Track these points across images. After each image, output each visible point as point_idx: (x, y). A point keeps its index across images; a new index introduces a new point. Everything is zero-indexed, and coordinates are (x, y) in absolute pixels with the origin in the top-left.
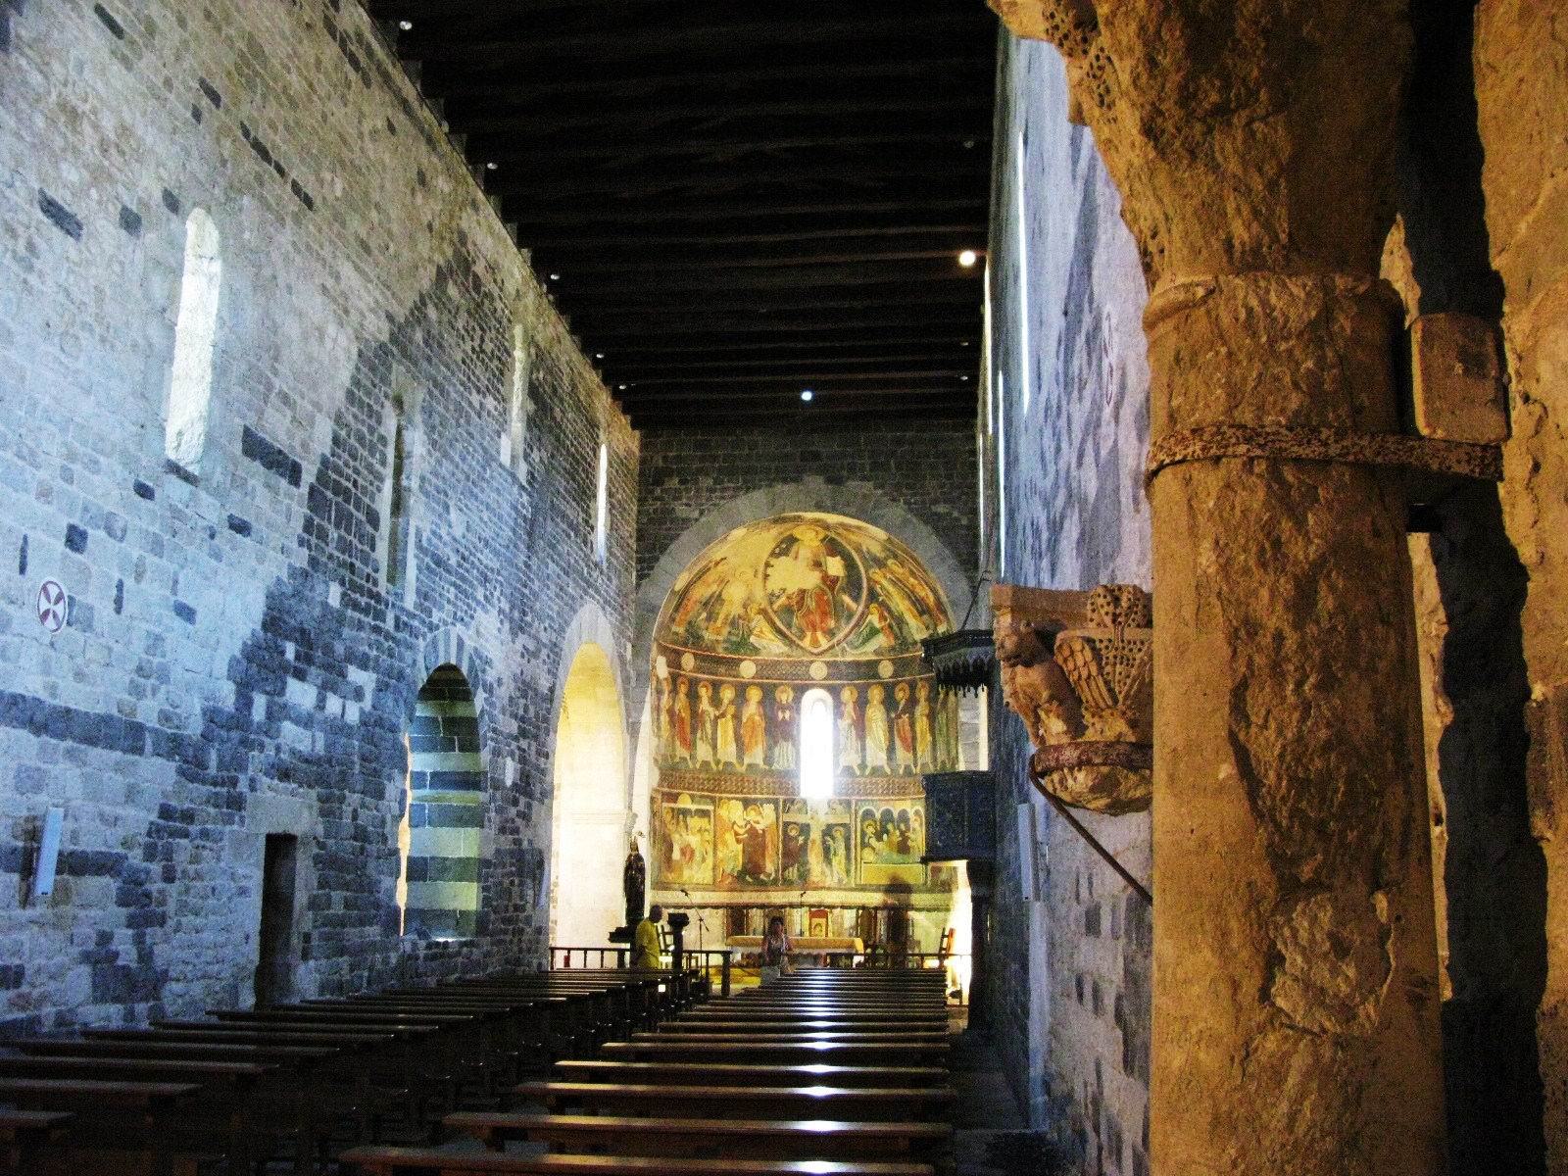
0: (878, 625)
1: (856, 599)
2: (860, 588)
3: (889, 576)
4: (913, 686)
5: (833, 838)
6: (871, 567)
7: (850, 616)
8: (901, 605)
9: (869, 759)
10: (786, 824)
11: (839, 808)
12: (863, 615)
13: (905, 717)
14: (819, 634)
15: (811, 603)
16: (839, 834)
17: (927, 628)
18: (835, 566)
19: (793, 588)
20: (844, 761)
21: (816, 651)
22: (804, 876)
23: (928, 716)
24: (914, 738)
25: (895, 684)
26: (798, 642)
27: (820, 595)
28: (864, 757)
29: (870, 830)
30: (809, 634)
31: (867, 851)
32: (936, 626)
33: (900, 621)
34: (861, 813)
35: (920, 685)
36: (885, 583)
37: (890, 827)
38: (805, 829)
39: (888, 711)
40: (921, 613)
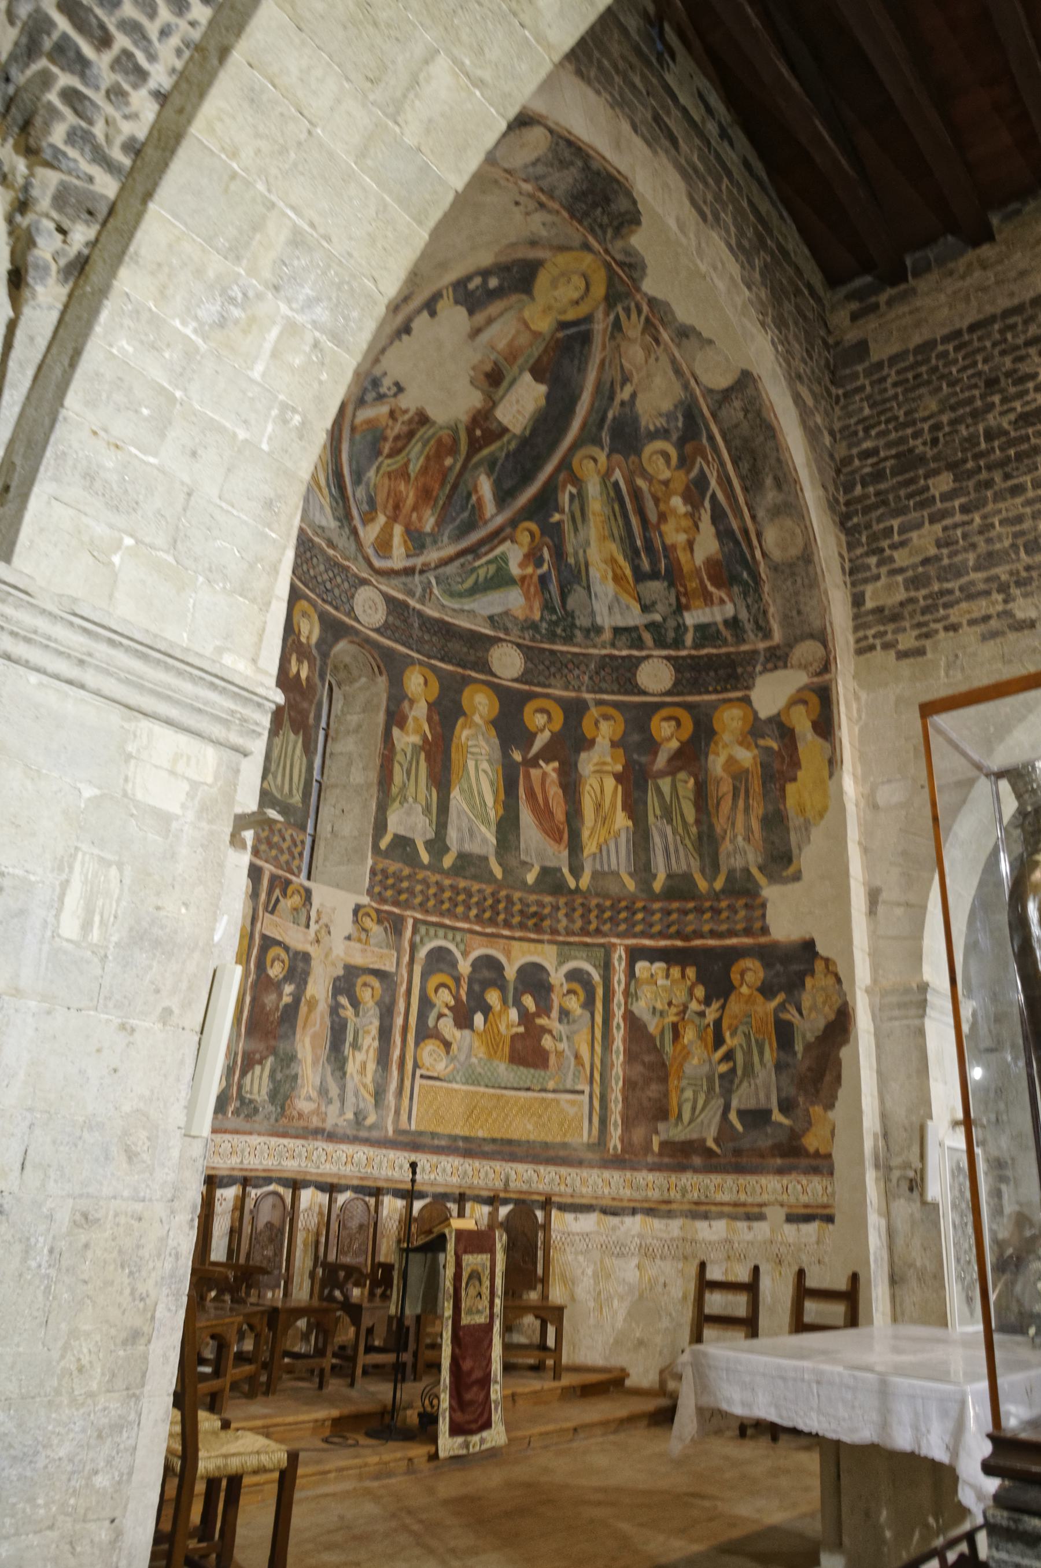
0: (515, 570)
1: (503, 497)
2: (527, 478)
3: (618, 475)
4: (574, 710)
5: (355, 1003)
6: (597, 442)
7: (470, 526)
8: (597, 549)
9: (452, 835)
10: (268, 942)
11: (376, 929)
12: (496, 537)
13: (551, 769)
14: (398, 530)
15: (416, 456)
16: (369, 994)
17: (645, 609)
18: (522, 402)
19: (408, 402)
20: (396, 823)
21: (378, 563)
22: (282, 1092)
23: (619, 778)
24: (574, 813)
25: (531, 696)
26: (357, 522)
27: (446, 447)
28: (441, 826)
29: (444, 998)
30: (382, 519)
31: (430, 1049)
32: (680, 609)
33: (573, 577)
34: (422, 953)
35: (594, 712)
36: (593, 488)
37: (493, 997)
38: (299, 967)
39: (505, 747)
40: (640, 576)
